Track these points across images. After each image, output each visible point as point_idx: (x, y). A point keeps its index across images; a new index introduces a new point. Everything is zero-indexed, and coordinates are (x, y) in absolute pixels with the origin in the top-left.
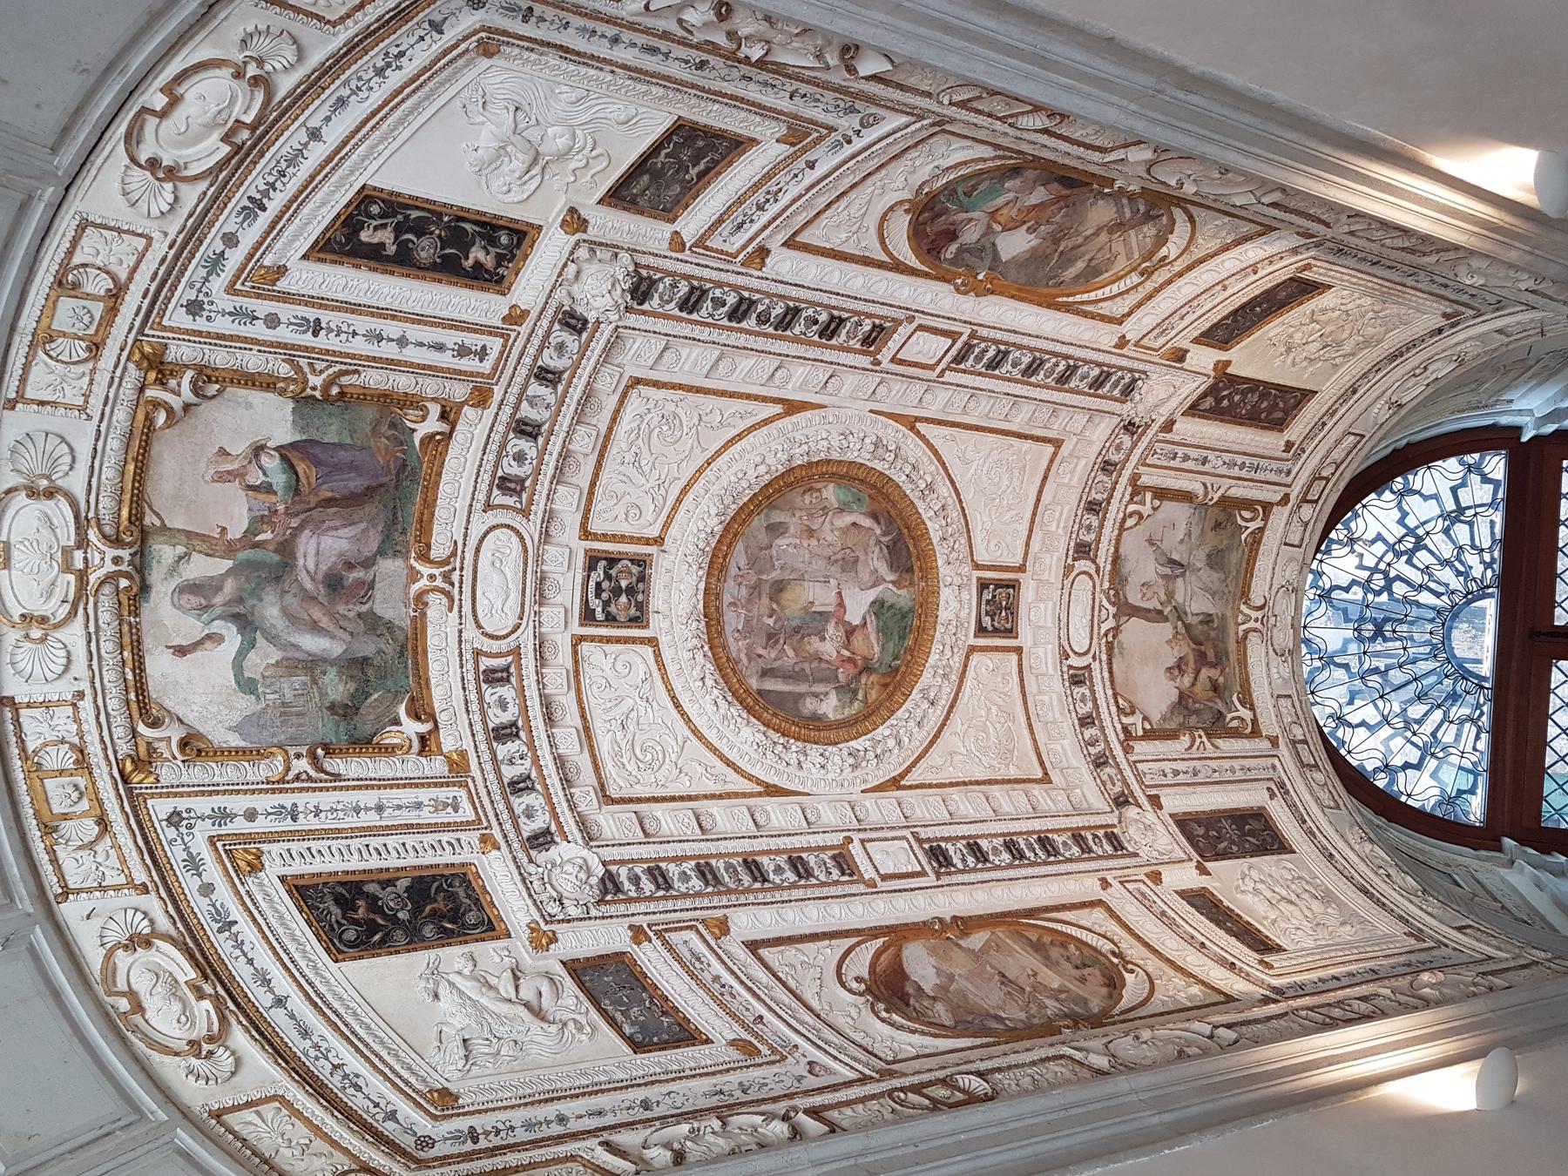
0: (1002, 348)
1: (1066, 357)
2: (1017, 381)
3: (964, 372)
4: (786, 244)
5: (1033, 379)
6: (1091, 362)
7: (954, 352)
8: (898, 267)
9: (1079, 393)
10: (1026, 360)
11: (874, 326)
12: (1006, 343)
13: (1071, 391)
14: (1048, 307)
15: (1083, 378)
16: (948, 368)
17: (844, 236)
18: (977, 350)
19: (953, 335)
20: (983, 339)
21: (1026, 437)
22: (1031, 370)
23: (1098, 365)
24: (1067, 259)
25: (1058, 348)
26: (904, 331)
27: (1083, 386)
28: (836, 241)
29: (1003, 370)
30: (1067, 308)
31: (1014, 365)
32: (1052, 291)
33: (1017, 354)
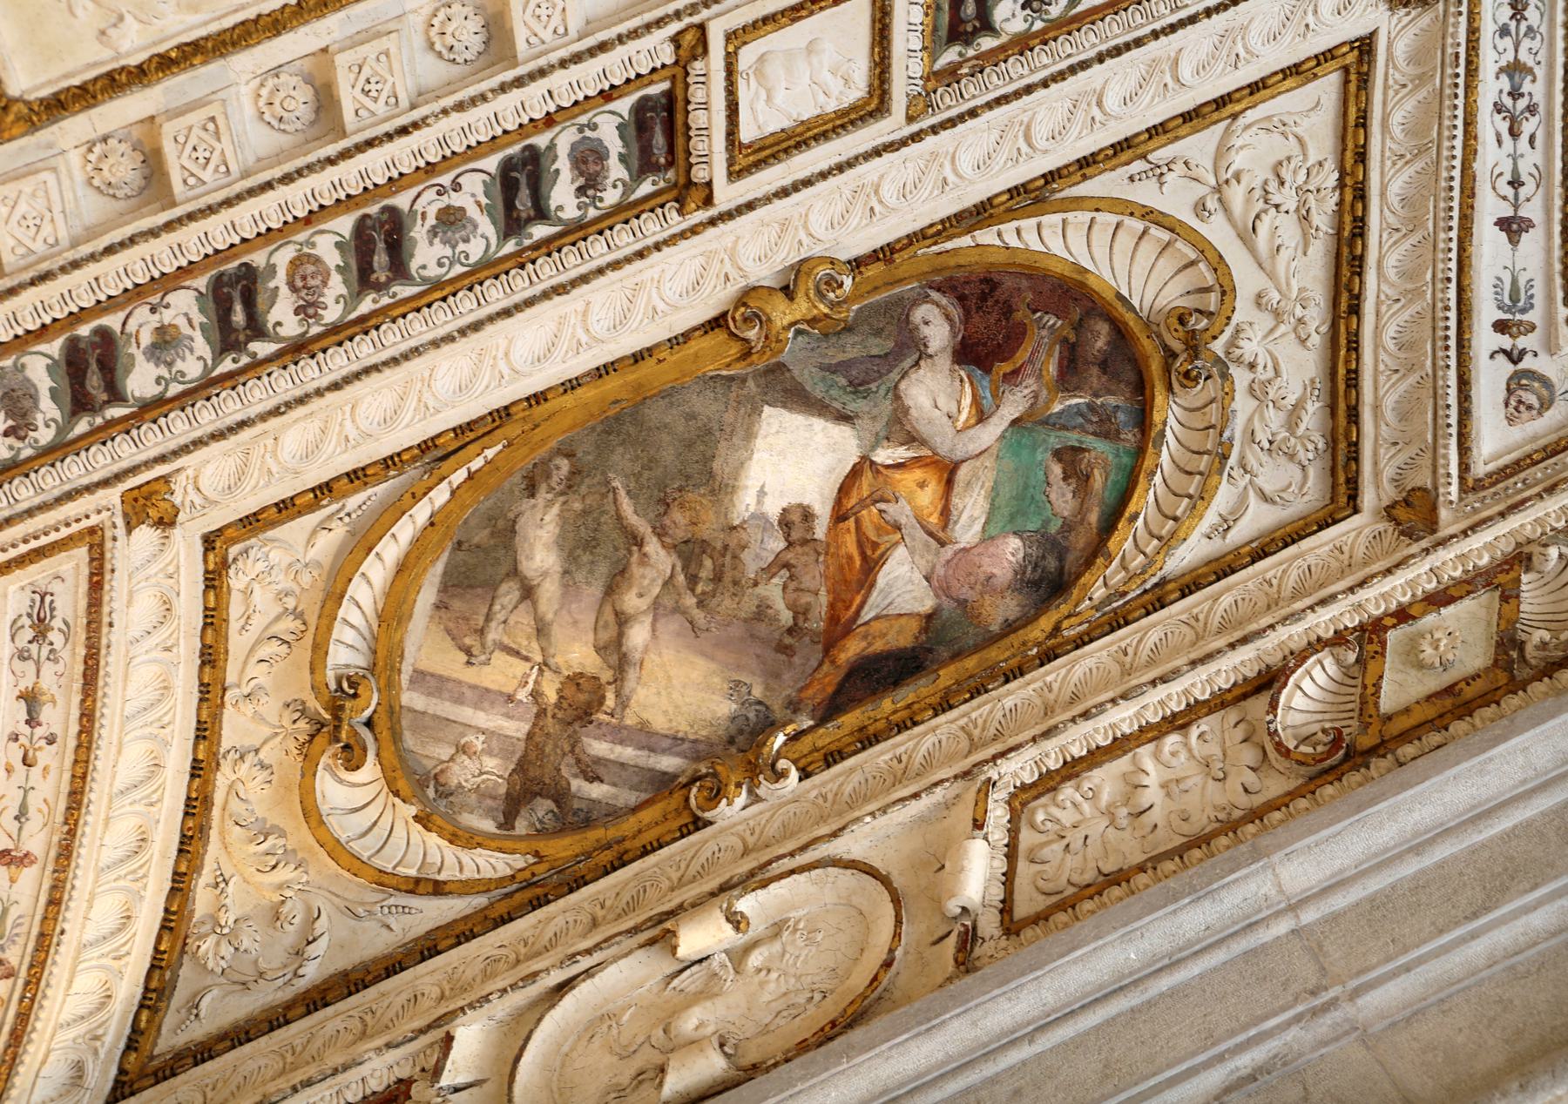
0: (540, 231)
1: (298, 349)
2: (396, 183)
3: (607, 95)
4: (1365, 46)
5: (344, 225)
6: (185, 400)
7: (708, 119)
8: (1032, 196)
9: (136, 294)
10: (427, 256)
11: (987, 27)
12: (548, 246)
13: (166, 283)
14: (503, 415)
15: (165, 343)
16: (680, 70)
17: (1239, 161)
18: (616, 171)
19: (748, 157)
20: (627, 211)
21: (165, 64)
22: (380, 244)
23: (153, 408)
24: (600, 550)
25: (364, 350)
26: (907, 67)
27: (143, 323)
28: (1253, 146)
29: (474, 185)
30: (434, 454)
31: (451, 220)
32: (525, 460)
33: (475, 250)
